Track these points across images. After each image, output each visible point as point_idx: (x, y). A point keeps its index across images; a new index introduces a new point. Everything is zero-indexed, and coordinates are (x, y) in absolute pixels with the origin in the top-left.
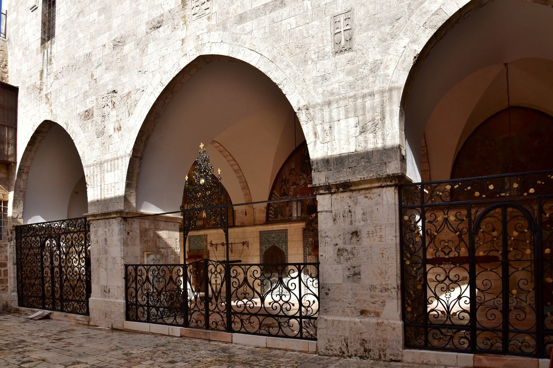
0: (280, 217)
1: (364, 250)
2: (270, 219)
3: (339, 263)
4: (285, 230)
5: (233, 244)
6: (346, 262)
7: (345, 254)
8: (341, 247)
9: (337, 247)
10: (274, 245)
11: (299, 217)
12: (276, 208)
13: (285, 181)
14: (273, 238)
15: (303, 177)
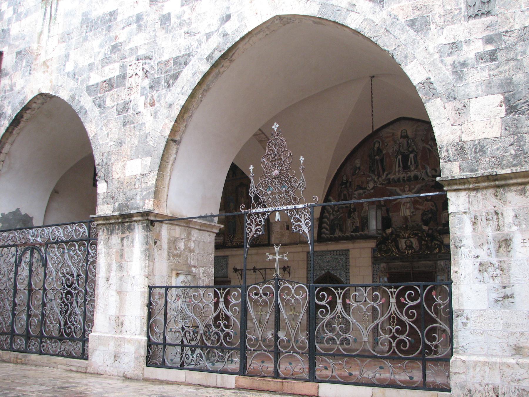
0: (338, 234)
1: (518, 263)
3: (482, 281)
4: (346, 250)
5: (267, 270)
6: (491, 280)
7: (491, 269)
8: (485, 261)
9: (479, 260)
10: (328, 272)
11: (379, 230)
12: (333, 220)
13: (346, 184)
14: (328, 262)
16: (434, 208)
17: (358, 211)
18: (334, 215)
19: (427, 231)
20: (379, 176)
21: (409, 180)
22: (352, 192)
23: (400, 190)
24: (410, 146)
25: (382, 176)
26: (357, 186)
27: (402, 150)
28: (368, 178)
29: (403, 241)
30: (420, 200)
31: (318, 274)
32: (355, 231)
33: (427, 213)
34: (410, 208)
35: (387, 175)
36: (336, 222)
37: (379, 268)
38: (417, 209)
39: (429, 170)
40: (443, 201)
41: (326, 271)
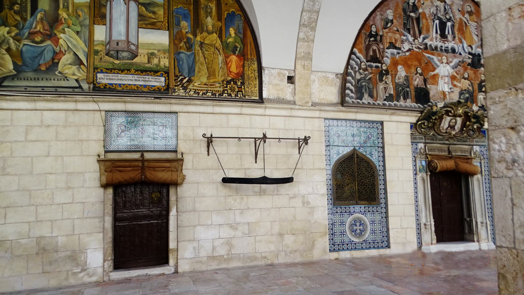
0: (366, 99)
2: (347, 99)
4: (377, 122)
12: (359, 81)
15: (407, 40)
16: (471, 88)
17: (392, 75)
18: (361, 74)
19: (475, 111)
20: (415, 38)
21: (446, 51)
22: (384, 48)
23: (439, 61)
24: (447, 13)
25: (419, 39)
26: (390, 43)
27: (439, 15)
28: (402, 37)
29: (449, 118)
30: (457, 76)
31: (341, 152)
32: (387, 99)
33: (464, 92)
34: (448, 83)
35: (424, 39)
36: (364, 84)
37: (416, 149)
38: (455, 86)
39: (465, 45)
40: (478, 82)
41: (352, 148)
